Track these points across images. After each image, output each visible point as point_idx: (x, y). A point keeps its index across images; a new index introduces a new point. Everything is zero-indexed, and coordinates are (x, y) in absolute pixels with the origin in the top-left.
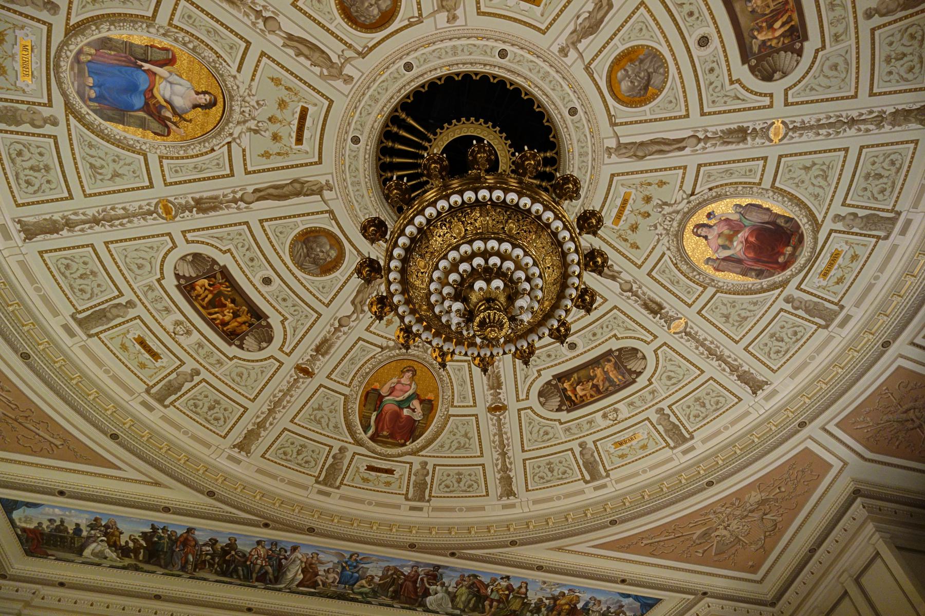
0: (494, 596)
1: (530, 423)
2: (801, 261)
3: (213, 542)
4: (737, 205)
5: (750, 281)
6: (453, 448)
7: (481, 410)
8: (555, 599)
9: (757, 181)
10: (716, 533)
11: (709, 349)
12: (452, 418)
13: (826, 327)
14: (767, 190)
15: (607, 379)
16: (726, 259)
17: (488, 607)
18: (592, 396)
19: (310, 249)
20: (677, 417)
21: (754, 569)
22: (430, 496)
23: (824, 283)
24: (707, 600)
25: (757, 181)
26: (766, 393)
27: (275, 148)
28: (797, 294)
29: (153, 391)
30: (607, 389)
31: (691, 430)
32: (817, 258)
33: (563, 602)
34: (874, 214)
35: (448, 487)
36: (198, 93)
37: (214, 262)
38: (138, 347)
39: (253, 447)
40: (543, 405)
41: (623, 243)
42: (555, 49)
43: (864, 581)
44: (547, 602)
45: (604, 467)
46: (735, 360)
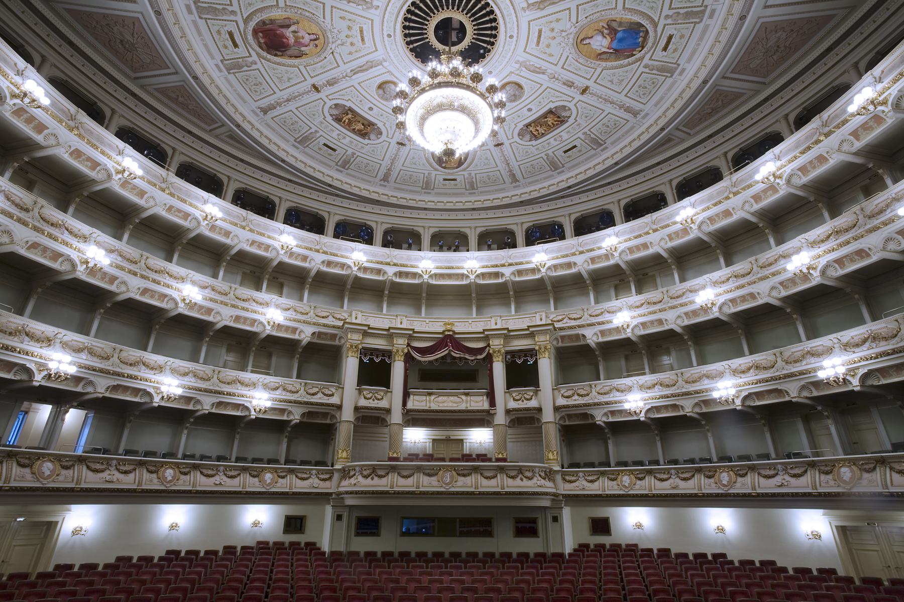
5: (264, 16)
16: (288, 26)
23: (226, 29)
27: (553, 25)
28: (232, 18)
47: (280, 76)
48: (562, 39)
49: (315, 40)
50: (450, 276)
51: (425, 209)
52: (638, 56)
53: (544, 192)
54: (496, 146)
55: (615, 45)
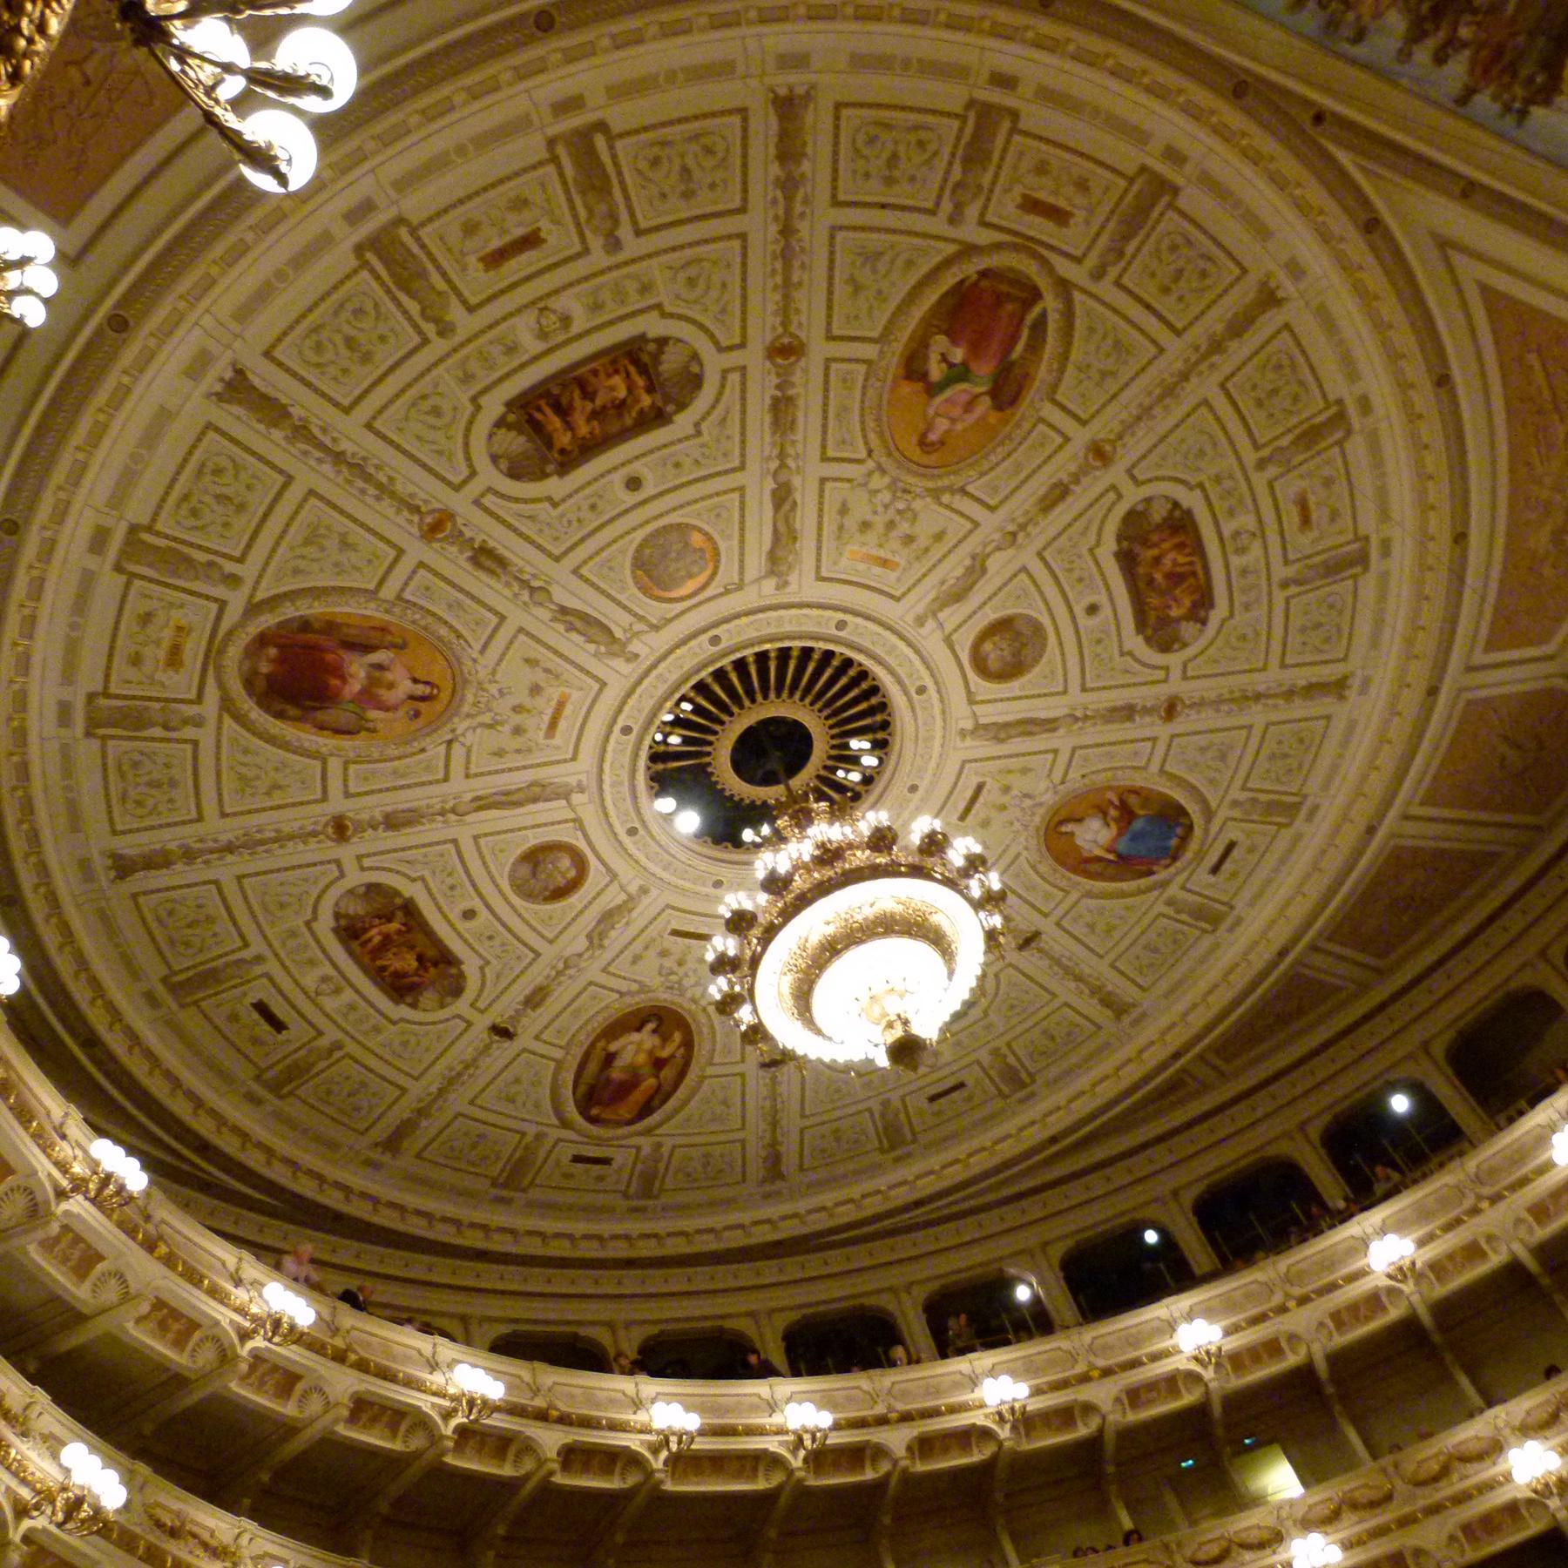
1: (724, 311)
2: (234, 652)
3: (1440, 59)
7: (819, 349)
11: (368, 478)
12: (875, 334)
13: (134, 529)
15: (563, 411)
16: (367, 648)
19: (1017, 654)
20: (405, 312)
29: (1339, 435)
31: (365, 274)
35: (921, 144)
36: (1072, 834)
37: (1148, 640)
38: (1314, 516)
39: (1251, 295)
40: (695, 357)
41: (549, 665)
42: (654, 892)
45: (561, 175)
46: (305, 453)
47: (249, 773)
48: (1019, 814)
49: (423, 699)
50: (717, 1462)
51: (481, 1255)
52: (1162, 875)
53: (846, 1215)
54: (764, 1065)
55: (1122, 846)
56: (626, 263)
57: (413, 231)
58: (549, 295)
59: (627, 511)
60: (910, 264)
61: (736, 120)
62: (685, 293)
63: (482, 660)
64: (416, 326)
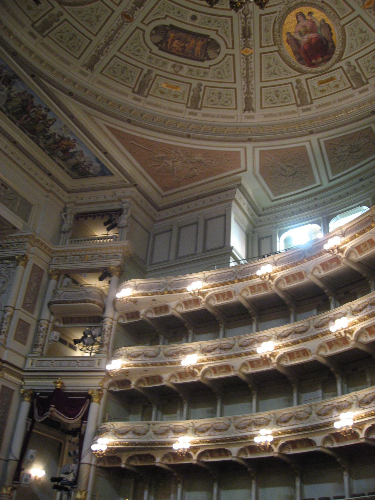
0: (33, 115)
1: (136, 39)
2: (319, 69)
4: (324, 20)
5: (293, 59)
6: (85, 19)
7: (119, 10)
8: (62, 138)
9: (341, 17)
10: (167, 161)
11: (247, 74)
13: (298, 106)
14: (340, 25)
15: (193, 49)
16: (296, 40)
17: (23, 118)
18: (178, 51)
21: (165, 189)
22: (47, 34)
23: (316, 86)
24: (134, 189)
25: (341, 17)
26: (249, 114)
30: (188, 54)
31: (203, 105)
32: (325, 73)
33: (65, 143)
34: (360, 75)
35: (61, 37)
40: (151, 35)
43: (209, 223)
44: (57, 137)
46: (253, 89)
56: (150, 66)
57: (187, 104)
58: (172, 74)
59: (203, 13)
60: (79, 12)
61: (103, 73)
62: (142, 50)
63: (279, 10)
64: (204, 90)
